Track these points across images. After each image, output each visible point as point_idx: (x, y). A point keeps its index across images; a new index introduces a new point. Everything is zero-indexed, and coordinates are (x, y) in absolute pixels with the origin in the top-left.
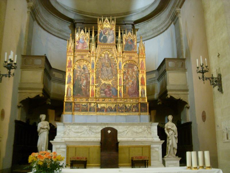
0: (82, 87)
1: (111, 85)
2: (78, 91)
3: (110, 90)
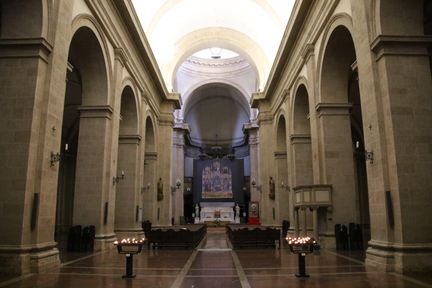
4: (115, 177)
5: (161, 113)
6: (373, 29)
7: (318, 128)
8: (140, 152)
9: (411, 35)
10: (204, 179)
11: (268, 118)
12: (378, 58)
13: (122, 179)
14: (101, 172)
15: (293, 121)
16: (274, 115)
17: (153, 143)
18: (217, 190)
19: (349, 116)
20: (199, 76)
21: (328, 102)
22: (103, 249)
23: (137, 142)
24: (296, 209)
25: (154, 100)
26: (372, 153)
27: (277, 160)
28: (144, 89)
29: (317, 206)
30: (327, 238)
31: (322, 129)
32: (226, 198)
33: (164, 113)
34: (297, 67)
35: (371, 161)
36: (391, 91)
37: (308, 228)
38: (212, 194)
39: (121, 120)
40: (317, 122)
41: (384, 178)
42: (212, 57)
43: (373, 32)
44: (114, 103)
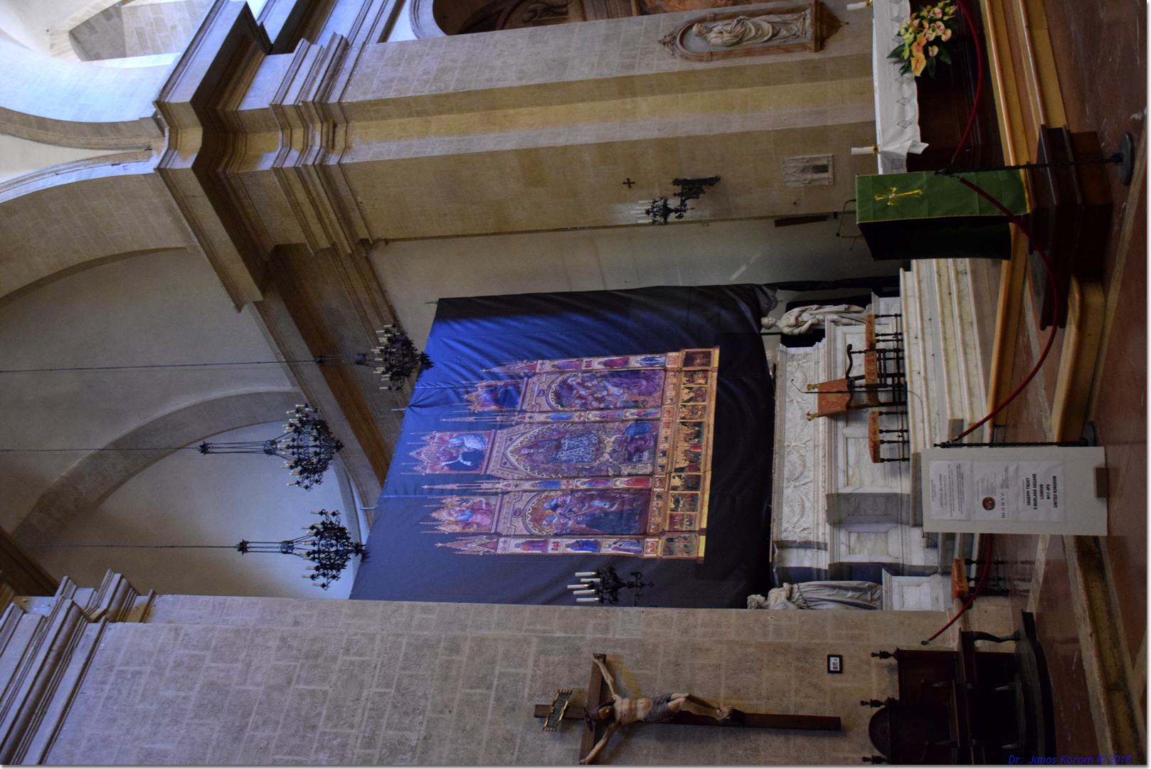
0: (613, 509)
1: (616, 439)
3: (632, 439)
10: (531, 544)
18: (639, 450)
32: (719, 383)
38: (676, 482)
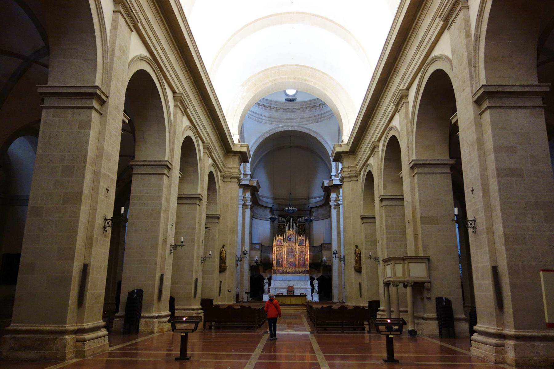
2: (279, 264)
4: (173, 244)
5: (225, 167)
6: (476, 77)
7: (413, 189)
8: (200, 214)
9: (522, 83)
11: (353, 174)
12: (481, 111)
13: (181, 246)
14: (156, 238)
15: (382, 179)
16: (360, 171)
17: (215, 203)
19: (450, 176)
20: (271, 122)
21: (425, 158)
22: (155, 332)
23: (198, 202)
24: (387, 284)
25: (217, 152)
26: (475, 221)
27: (364, 224)
28: (206, 139)
29: (412, 282)
30: (425, 321)
31: (416, 190)
33: (229, 168)
34: (388, 115)
35: (474, 231)
36: (497, 150)
37: (401, 309)
39: (181, 177)
40: (411, 182)
41: (489, 251)
42: (286, 100)
43: (476, 80)
44: (173, 158)
